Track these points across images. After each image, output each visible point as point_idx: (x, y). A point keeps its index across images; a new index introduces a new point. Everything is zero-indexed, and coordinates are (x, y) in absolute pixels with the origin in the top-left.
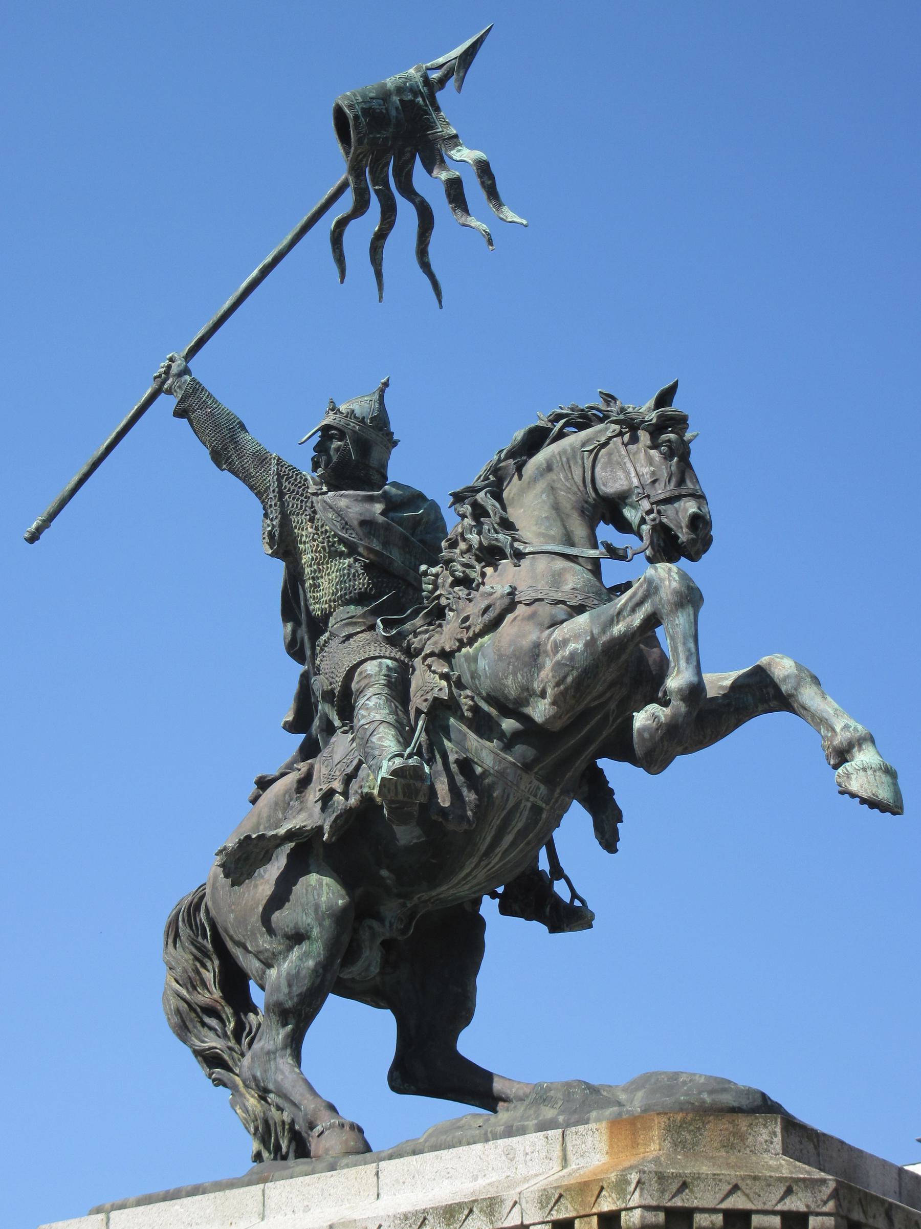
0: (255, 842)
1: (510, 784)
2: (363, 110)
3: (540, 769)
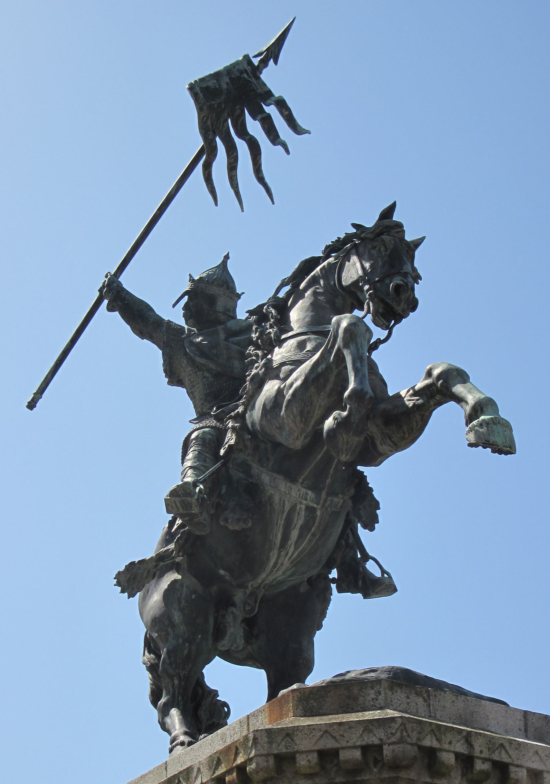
0: (138, 566)
1: (283, 493)
2: (202, 89)
3: (304, 480)
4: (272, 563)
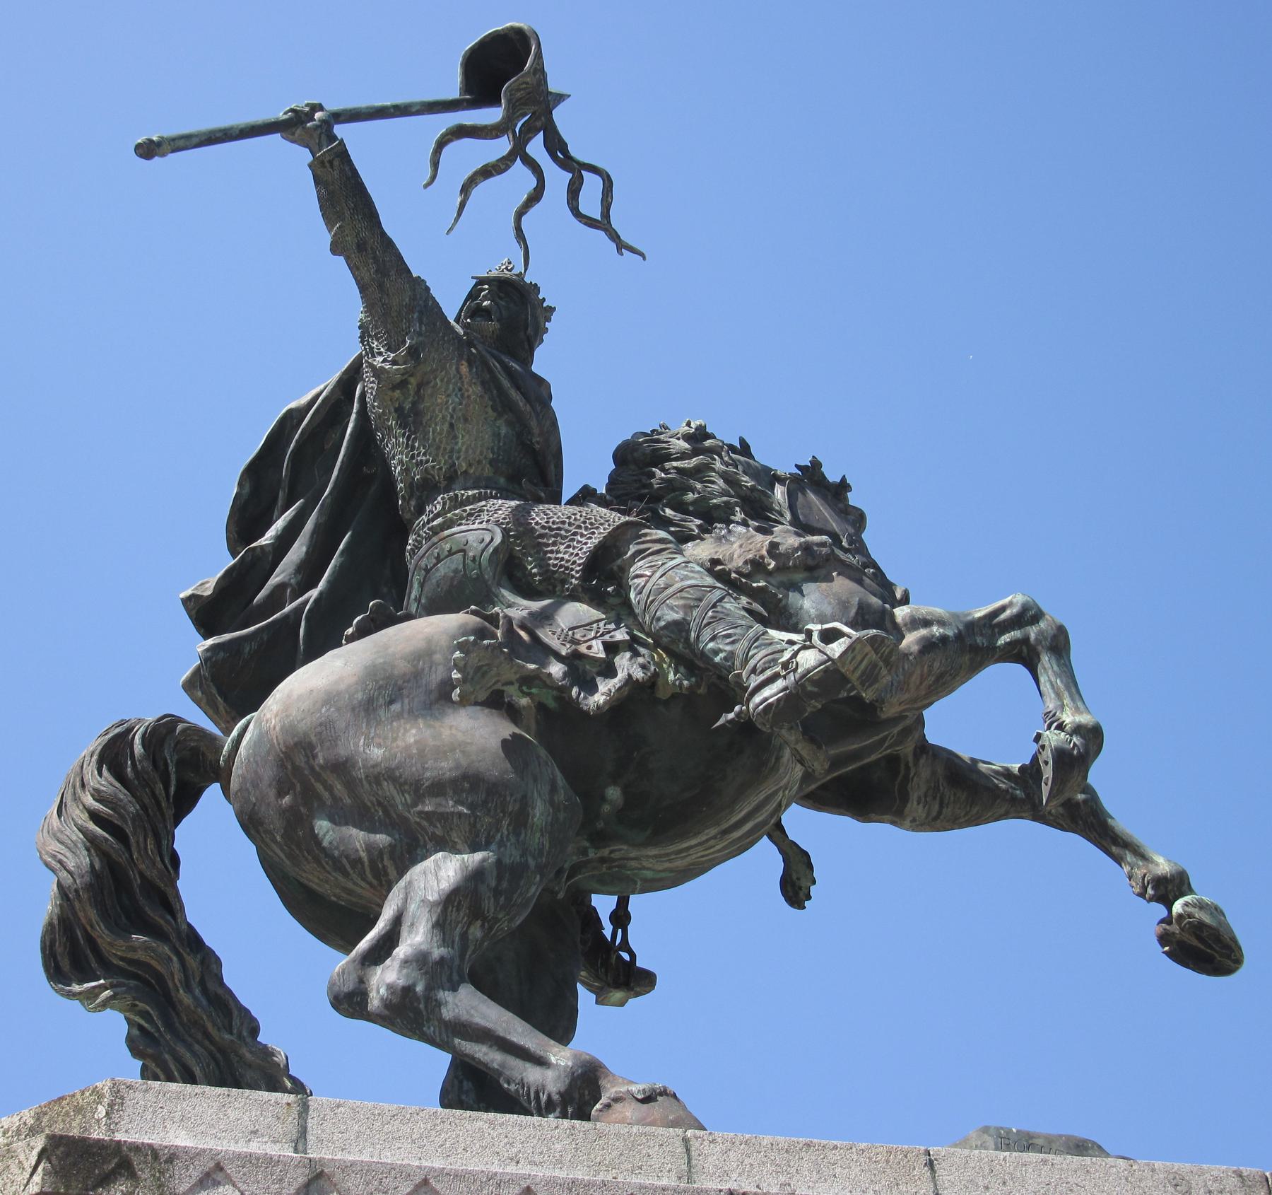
4: (685, 845)
